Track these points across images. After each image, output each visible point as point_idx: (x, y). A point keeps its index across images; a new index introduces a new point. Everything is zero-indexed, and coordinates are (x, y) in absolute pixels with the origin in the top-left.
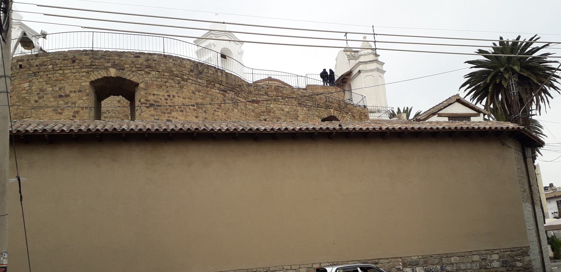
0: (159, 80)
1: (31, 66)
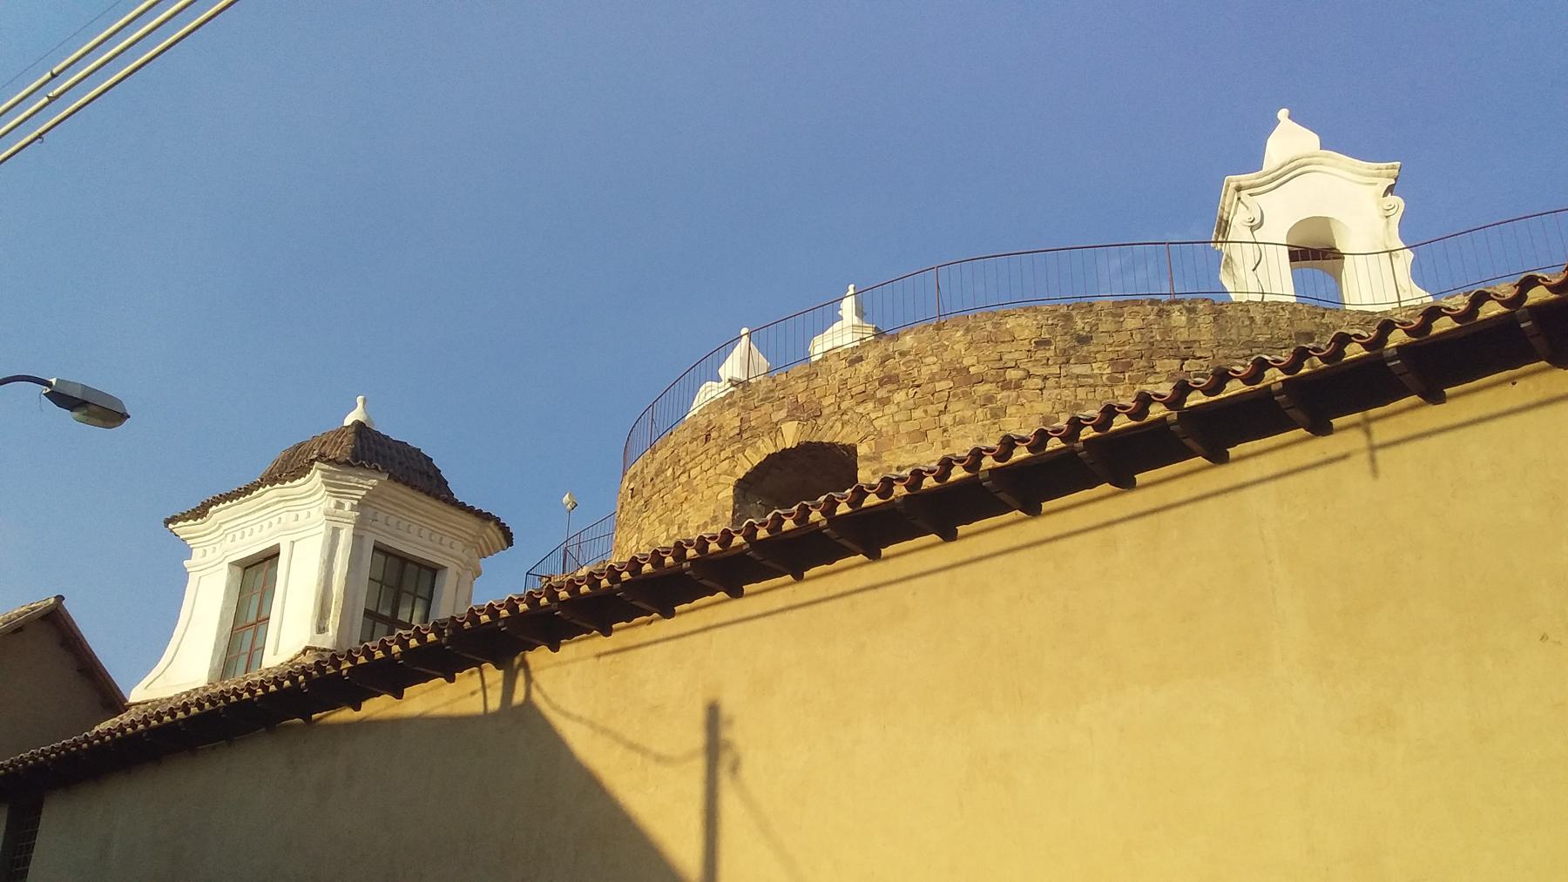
0: (918, 413)
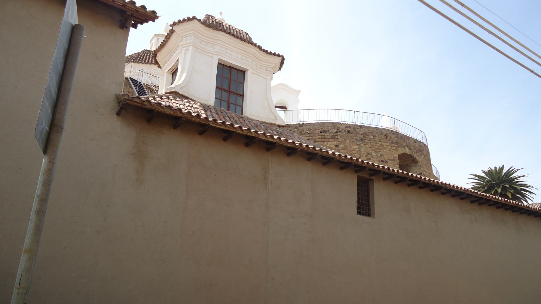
1: (357, 134)
